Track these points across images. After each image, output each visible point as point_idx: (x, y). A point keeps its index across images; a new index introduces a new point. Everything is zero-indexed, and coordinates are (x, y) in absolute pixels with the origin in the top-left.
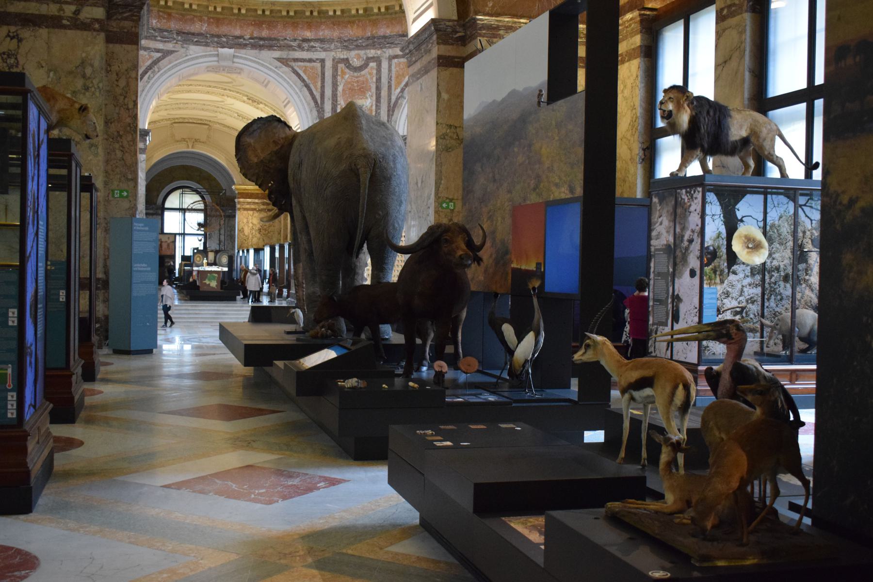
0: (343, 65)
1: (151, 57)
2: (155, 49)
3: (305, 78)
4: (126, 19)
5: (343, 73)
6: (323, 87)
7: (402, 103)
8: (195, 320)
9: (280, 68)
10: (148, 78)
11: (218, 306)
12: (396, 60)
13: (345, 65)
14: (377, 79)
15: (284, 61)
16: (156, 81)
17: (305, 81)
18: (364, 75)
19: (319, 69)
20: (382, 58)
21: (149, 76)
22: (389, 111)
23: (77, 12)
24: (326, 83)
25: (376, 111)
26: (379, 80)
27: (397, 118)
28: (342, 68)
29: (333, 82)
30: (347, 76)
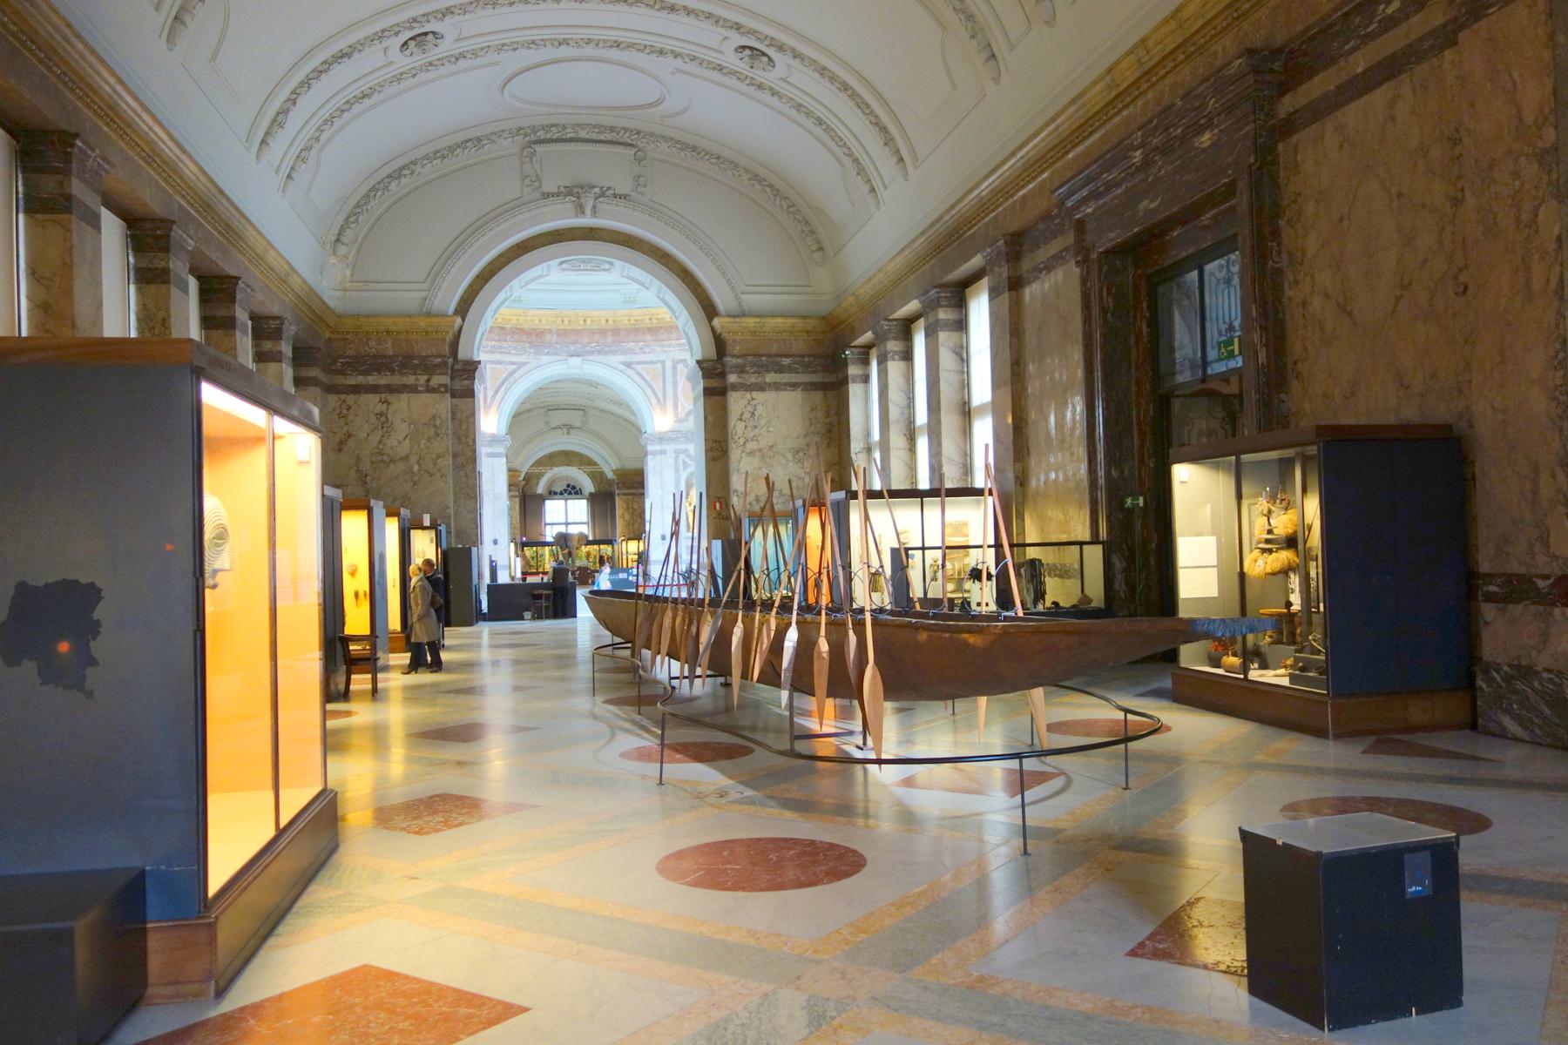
4: (466, 379)
6: (664, 386)
15: (628, 365)
23: (428, 380)
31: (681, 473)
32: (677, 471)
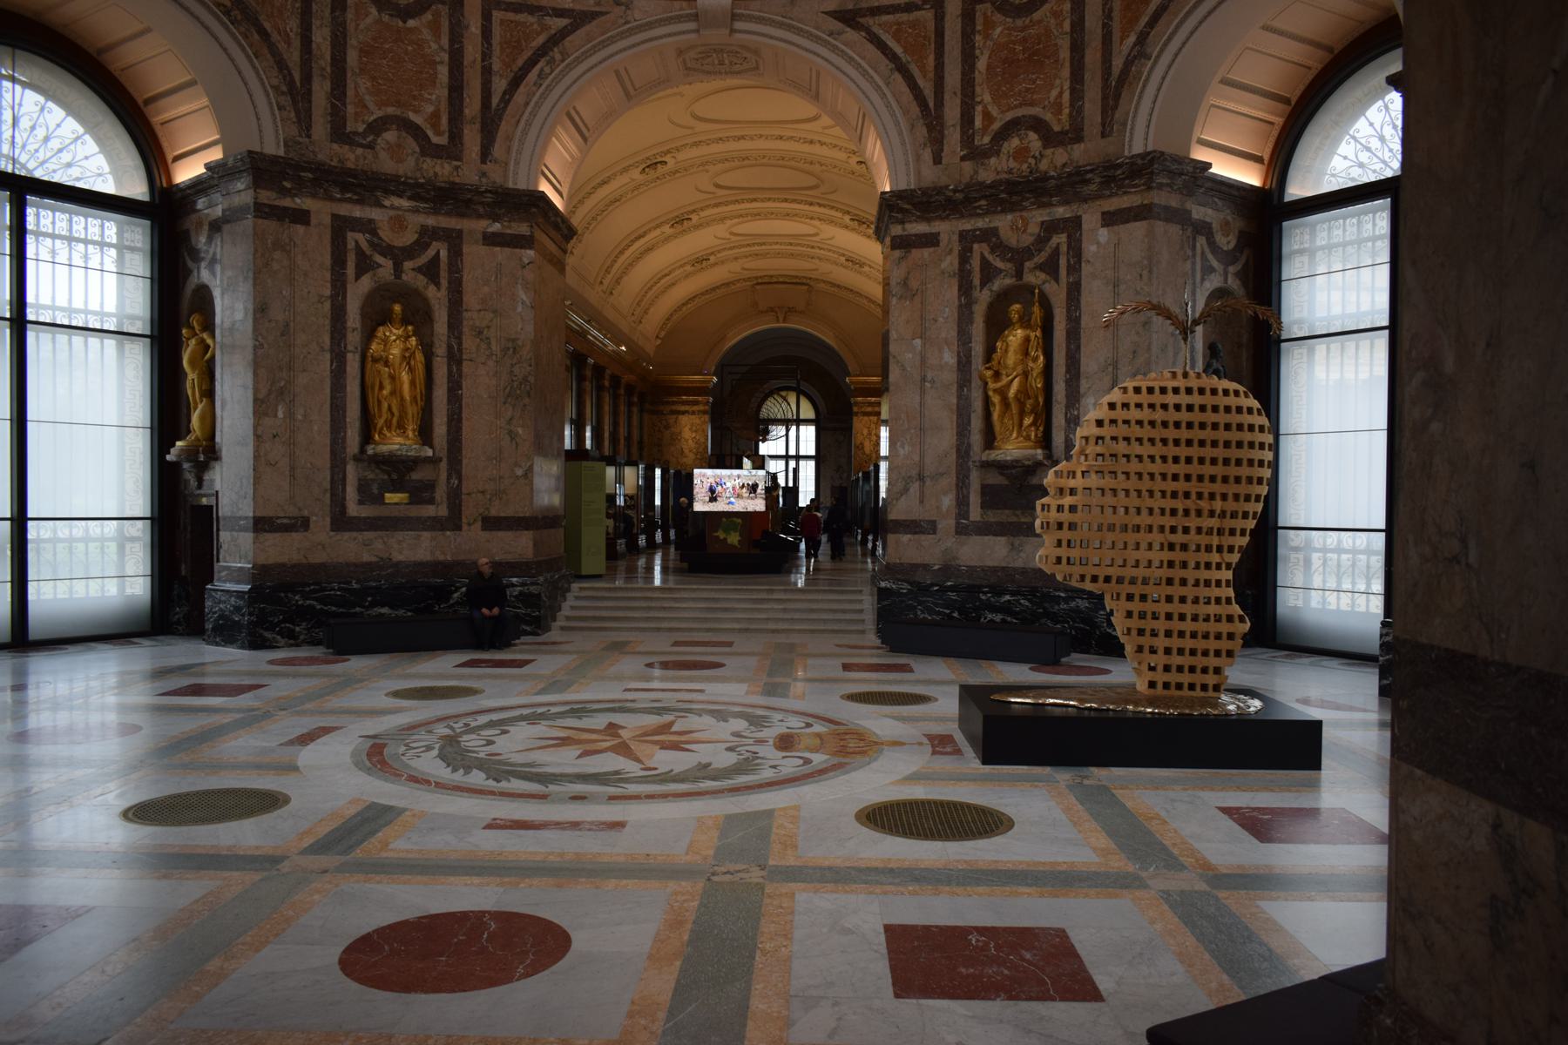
0: (988, 5)
1: (545, 28)
2: (554, 9)
3: (898, 50)
5: (990, 25)
7: (1140, 73)
8: (653, 625)
9: (839, 34)
10: (539, 76)
11: (716, 590)
13: (993, 4)
14: (1072, 25)
16: (557, 80)
17: (899, 59)
18: (1040, 22)
19: (931, 26)
21: (542, 70)
22: (1105, 98)
24: (946, 55)
25: (1072, 106)
26: (1078, 25)
27: (1128, 114)
28: (985, 14)
29: (963, 51)
30: (998, 30)
31: (976, 293)
32: (965, 289)
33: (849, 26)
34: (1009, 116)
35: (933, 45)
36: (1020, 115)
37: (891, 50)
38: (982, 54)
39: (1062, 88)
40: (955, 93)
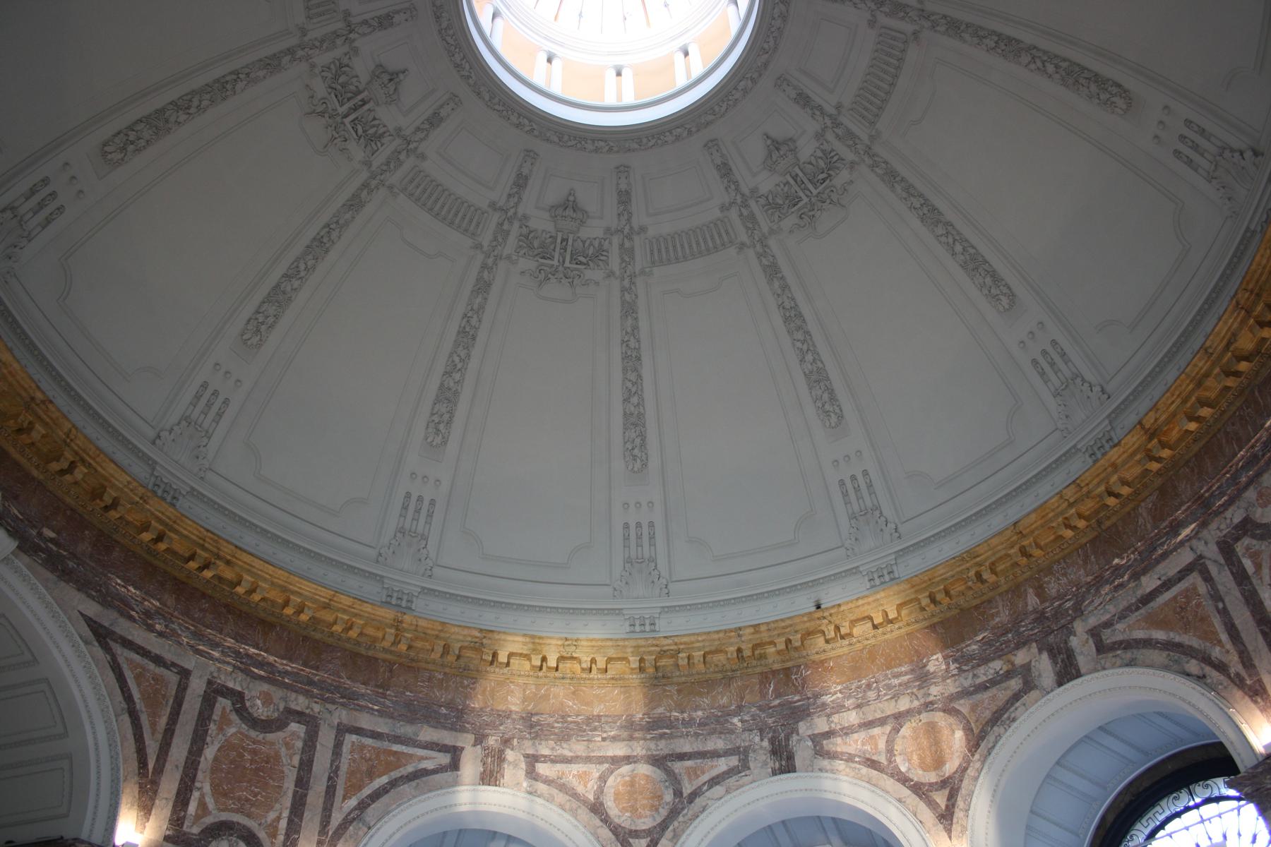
3: (136, 696)
5: (225, 721)
6: (169, 732)
12: (354, 737)
13: (233, 704)
15: (102, 635)
17: (134, 704)
18: (272, 744)
19: (172, 690)
20: (322, 722)
25: (287, 835)
26: (306, 766)
28: (224, 708)
29: (195, 731)
30: (232, 730)
33: (99, 642)
34: (225, 816)
35: (169, 710)
36: (235, 820)
37: (129, 690)
38: (212, 743)
39: (281, 814)
40: (177, 766)
